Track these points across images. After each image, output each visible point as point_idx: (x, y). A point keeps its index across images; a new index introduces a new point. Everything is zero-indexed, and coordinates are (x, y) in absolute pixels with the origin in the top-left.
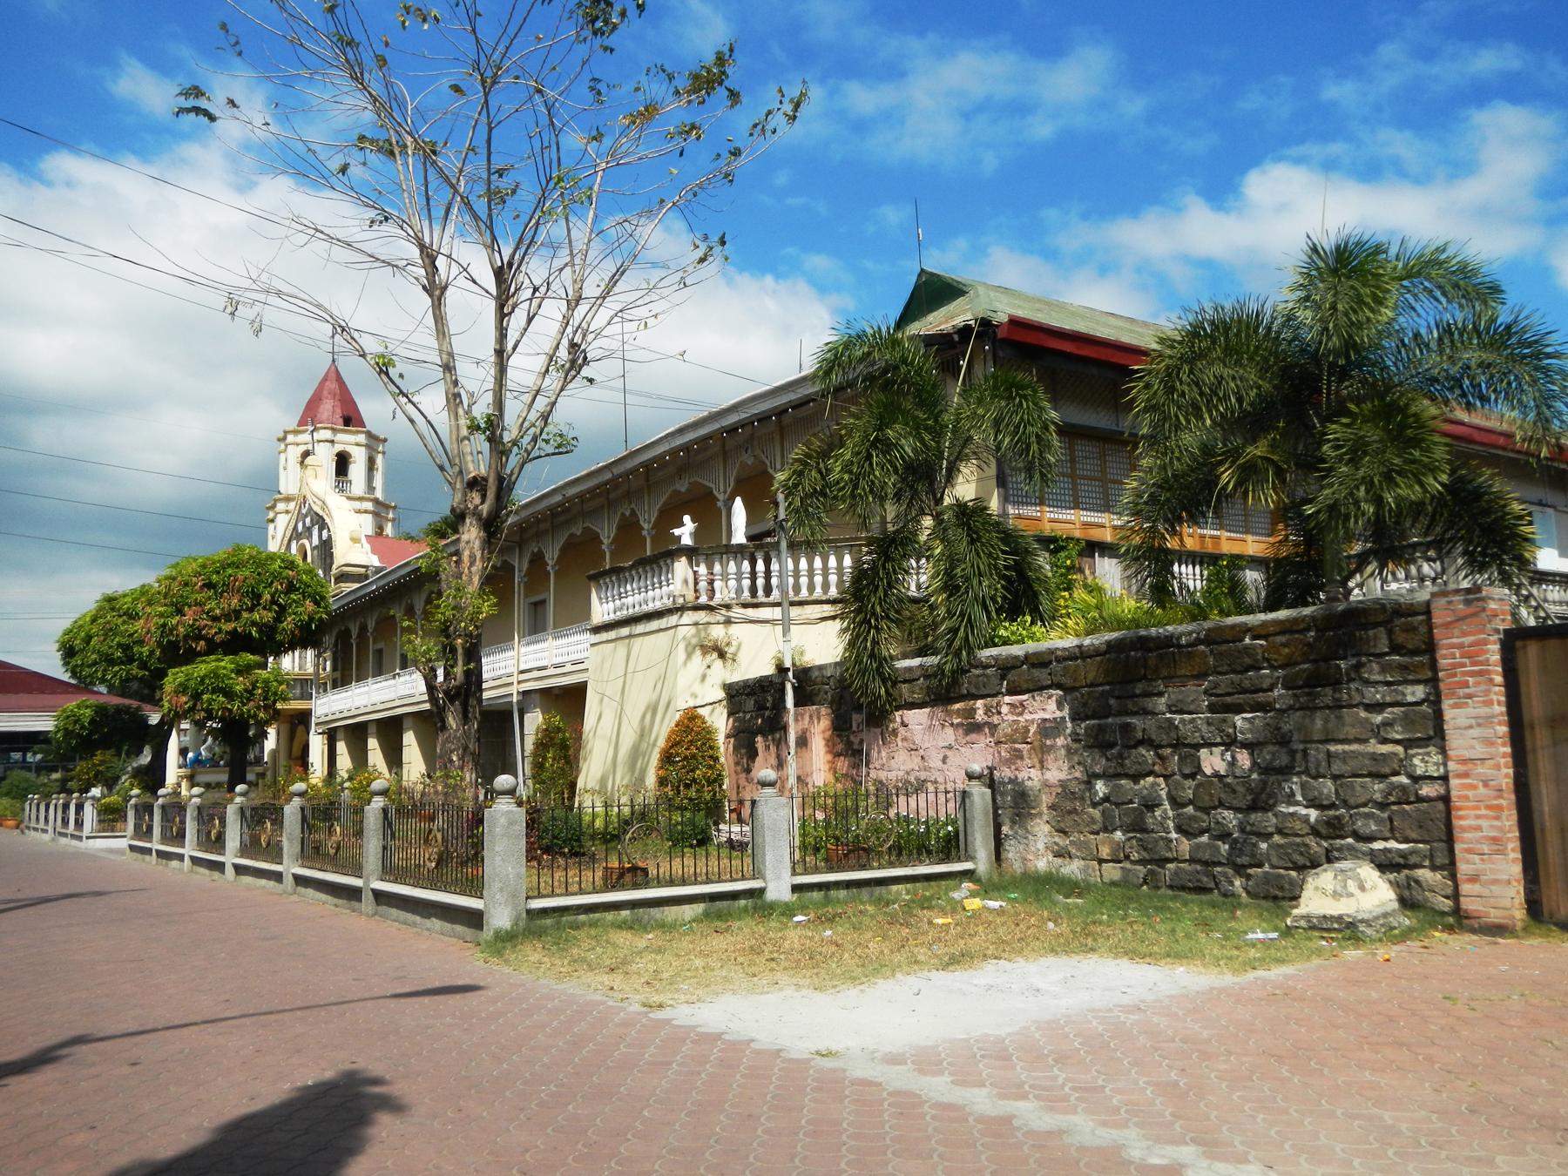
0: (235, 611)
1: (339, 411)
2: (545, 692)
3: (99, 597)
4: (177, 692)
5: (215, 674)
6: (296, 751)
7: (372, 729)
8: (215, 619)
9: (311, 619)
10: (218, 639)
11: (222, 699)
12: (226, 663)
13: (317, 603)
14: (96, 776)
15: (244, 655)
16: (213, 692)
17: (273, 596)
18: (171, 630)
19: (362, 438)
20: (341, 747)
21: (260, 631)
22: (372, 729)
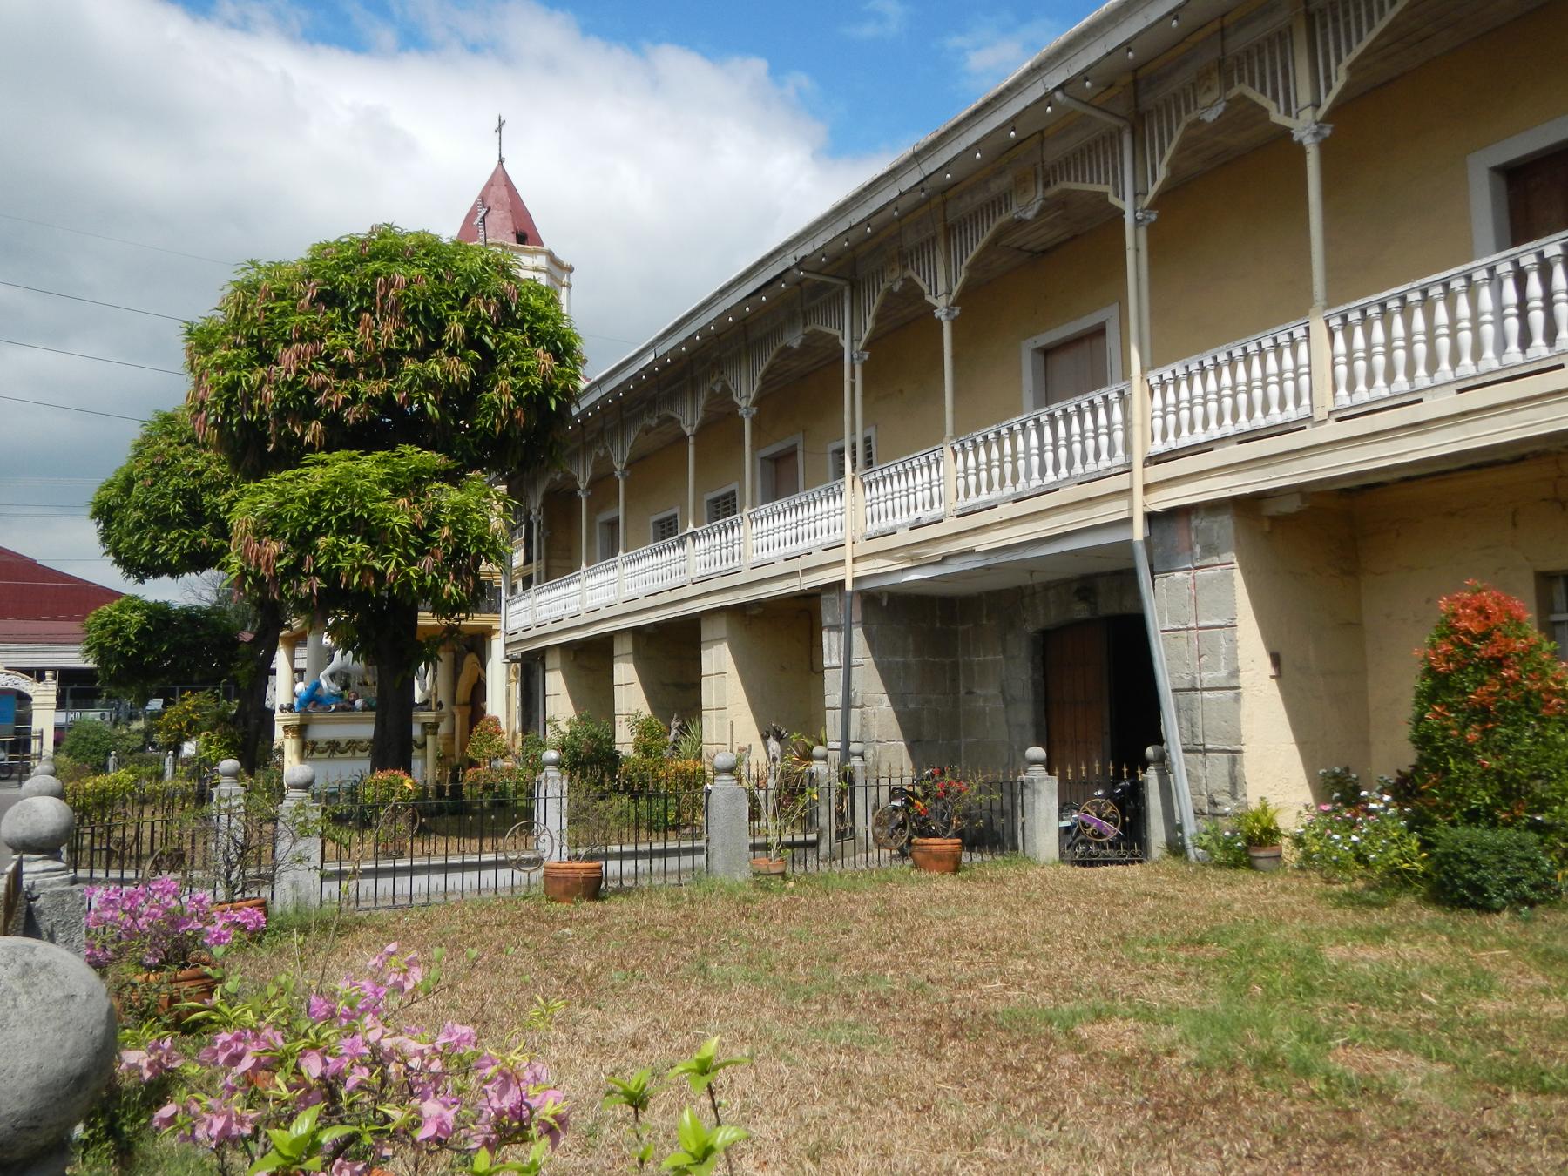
0: (388, 352)
1: (510, 224)
2: (1245, 507)
3: (149, 416)
4: (259, 533)
5: (339, 485)
6: (463, 692)
7: (623, 647)
8: (344, 371)
9: (549, 388)
10: (351, 415)
11: (360, 546)
12: (371, 466)
13: (558, 356)
14: (189, 725)
15: (407, 449)
16: (340, 532)
17: (469, 331)
18: (248, 398)
19: (541, 261)
20: (555, 682)
21: (442, 405)
22: (623, 647)
